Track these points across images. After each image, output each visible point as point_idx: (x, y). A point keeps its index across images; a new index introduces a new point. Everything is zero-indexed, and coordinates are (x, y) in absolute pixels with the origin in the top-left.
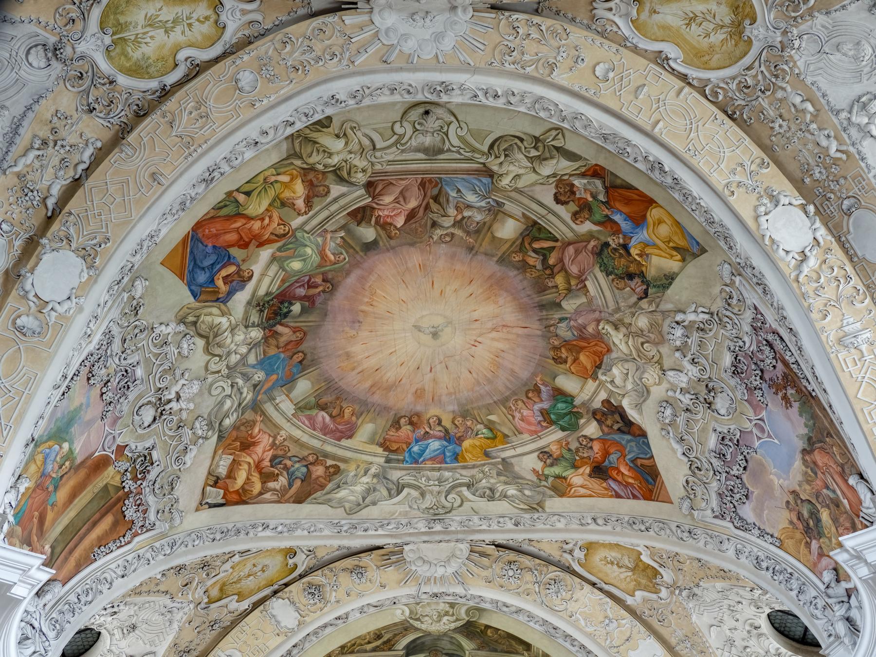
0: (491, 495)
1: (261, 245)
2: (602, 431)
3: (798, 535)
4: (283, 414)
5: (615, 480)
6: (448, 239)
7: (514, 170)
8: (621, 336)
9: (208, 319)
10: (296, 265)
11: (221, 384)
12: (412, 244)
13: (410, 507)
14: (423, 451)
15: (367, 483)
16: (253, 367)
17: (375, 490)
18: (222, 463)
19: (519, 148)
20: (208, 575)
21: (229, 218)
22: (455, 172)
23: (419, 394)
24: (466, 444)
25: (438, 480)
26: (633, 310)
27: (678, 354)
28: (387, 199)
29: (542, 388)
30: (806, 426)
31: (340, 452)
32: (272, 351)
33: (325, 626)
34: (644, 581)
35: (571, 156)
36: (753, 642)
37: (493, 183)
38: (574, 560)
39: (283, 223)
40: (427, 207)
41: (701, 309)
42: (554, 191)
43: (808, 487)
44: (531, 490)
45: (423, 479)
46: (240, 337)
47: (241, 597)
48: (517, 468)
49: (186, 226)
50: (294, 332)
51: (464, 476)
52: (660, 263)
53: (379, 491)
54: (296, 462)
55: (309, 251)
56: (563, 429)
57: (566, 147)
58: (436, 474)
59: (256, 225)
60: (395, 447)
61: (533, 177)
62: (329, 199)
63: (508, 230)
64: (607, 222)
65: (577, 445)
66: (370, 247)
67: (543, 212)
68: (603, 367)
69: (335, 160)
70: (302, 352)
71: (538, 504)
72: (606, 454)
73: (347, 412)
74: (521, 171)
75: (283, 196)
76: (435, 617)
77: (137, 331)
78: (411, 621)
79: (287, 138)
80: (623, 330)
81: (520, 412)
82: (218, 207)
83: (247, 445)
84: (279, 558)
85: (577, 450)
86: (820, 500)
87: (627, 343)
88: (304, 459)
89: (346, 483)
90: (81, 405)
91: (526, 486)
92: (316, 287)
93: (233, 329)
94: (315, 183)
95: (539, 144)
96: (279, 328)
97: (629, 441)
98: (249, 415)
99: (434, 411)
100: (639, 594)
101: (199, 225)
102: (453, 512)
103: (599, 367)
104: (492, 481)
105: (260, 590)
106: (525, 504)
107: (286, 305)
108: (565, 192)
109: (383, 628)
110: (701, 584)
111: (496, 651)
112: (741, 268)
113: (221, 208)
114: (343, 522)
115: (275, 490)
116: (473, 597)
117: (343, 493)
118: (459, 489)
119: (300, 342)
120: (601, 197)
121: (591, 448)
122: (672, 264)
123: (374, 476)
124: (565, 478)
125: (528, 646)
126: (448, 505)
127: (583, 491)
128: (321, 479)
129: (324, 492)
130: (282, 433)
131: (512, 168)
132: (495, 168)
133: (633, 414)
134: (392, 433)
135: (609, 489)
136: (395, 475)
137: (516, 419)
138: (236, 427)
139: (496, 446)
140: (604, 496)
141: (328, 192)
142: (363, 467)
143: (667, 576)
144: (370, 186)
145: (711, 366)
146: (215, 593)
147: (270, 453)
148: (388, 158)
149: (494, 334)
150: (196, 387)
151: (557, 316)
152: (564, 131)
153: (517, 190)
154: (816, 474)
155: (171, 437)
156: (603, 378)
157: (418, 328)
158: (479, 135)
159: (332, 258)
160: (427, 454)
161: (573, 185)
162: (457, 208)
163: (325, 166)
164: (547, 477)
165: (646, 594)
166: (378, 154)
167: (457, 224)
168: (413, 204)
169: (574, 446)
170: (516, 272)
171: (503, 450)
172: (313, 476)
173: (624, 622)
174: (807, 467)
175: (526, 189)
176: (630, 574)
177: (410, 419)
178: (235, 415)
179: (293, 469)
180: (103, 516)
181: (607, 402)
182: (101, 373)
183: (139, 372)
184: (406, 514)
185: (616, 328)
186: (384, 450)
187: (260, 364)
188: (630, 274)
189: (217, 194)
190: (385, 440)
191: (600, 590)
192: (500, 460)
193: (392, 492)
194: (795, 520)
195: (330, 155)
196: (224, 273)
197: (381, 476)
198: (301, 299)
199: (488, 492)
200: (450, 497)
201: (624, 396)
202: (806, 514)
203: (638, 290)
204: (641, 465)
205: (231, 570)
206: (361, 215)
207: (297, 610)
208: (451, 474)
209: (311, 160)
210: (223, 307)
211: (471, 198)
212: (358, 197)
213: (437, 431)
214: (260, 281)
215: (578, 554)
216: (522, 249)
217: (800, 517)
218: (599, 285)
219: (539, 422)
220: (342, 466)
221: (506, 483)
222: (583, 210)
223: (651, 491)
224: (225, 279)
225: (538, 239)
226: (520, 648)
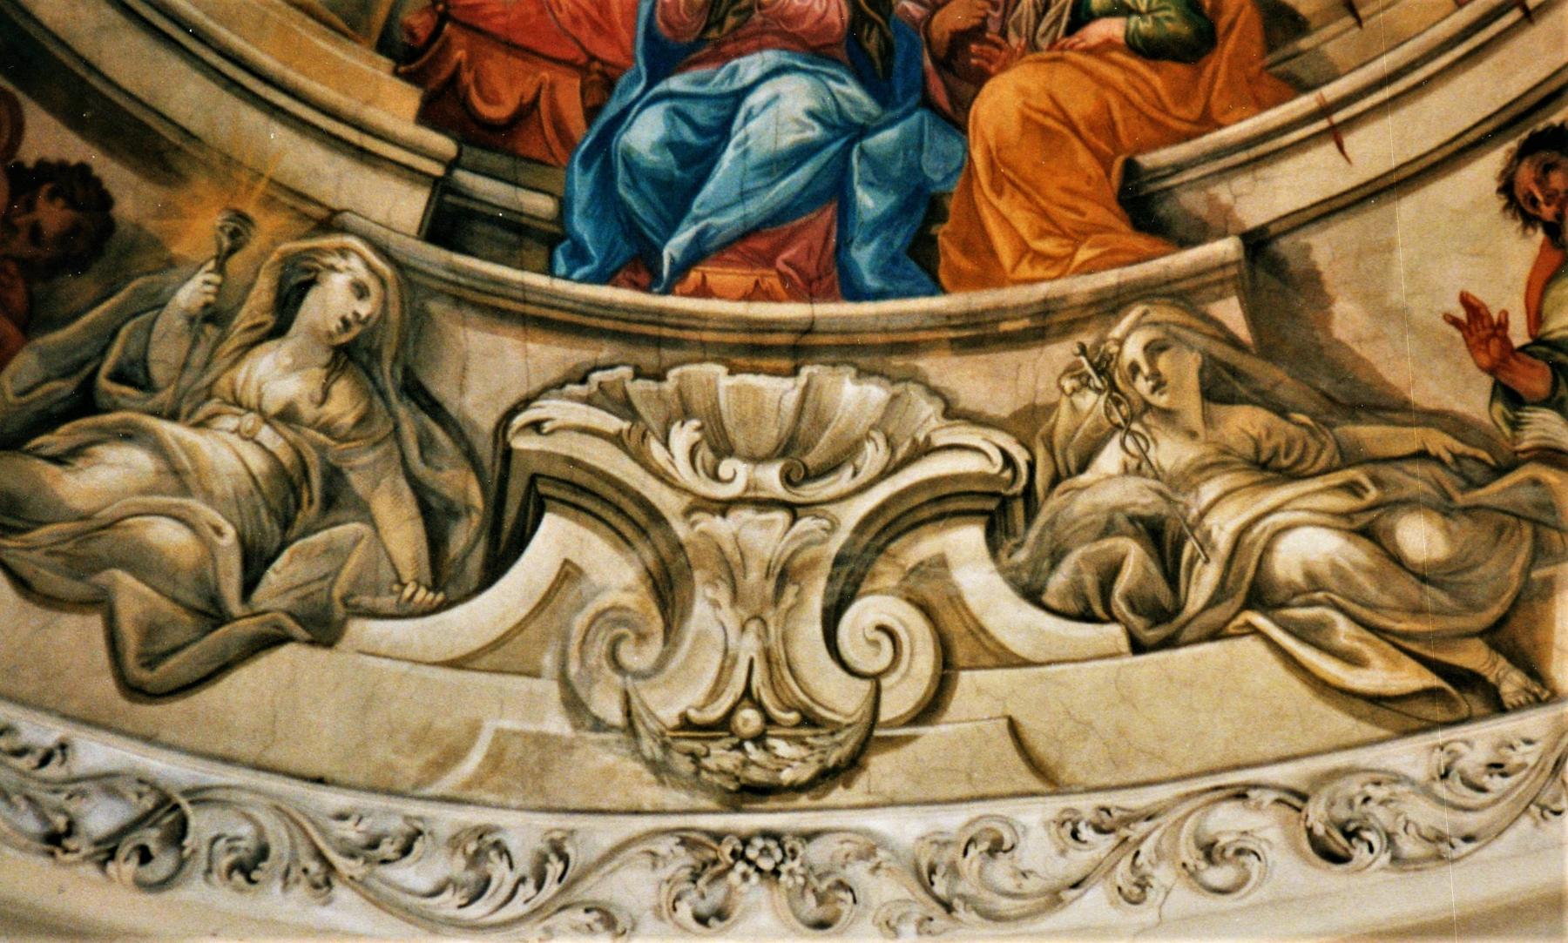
13: (574, 704)
14: (696, 159)
15: (287, 416)
17: (337, 497)
24: (1000, 103)
25: (787, 447)
44: (1445, 509)
45: (683, 436)
48: (1348, 319)
53: (364, 511)
58: (777, 392)
60: (501, 91)
71: (1496, 635)
91: (1416, 480)
102: (880, 765)
104: (1171, 452)
114: (96, 752)
117: (108, 475)
118: (926, 546)
123: (349, 355)
126: (841, 697)
139: (1207, 122)
142: (273, 236)
160: (723, 197)
171: (1259, 154)
184: (524, 767)
192: (1226, 248)
193: (461, 536)
199: (1134, 557)
208: (876, 393)
220: (131, 195)
221: (1269, 468)
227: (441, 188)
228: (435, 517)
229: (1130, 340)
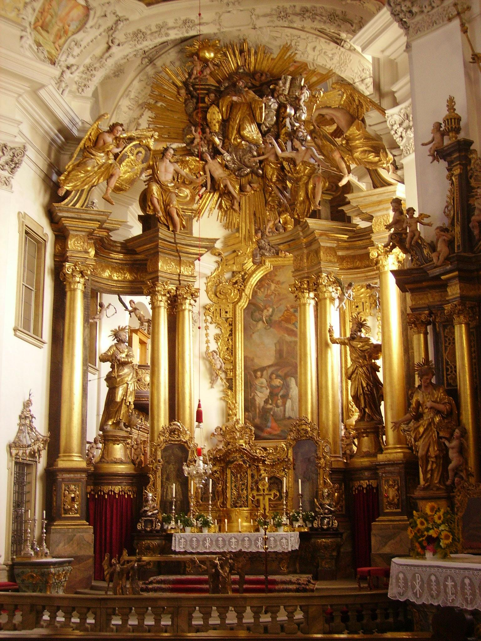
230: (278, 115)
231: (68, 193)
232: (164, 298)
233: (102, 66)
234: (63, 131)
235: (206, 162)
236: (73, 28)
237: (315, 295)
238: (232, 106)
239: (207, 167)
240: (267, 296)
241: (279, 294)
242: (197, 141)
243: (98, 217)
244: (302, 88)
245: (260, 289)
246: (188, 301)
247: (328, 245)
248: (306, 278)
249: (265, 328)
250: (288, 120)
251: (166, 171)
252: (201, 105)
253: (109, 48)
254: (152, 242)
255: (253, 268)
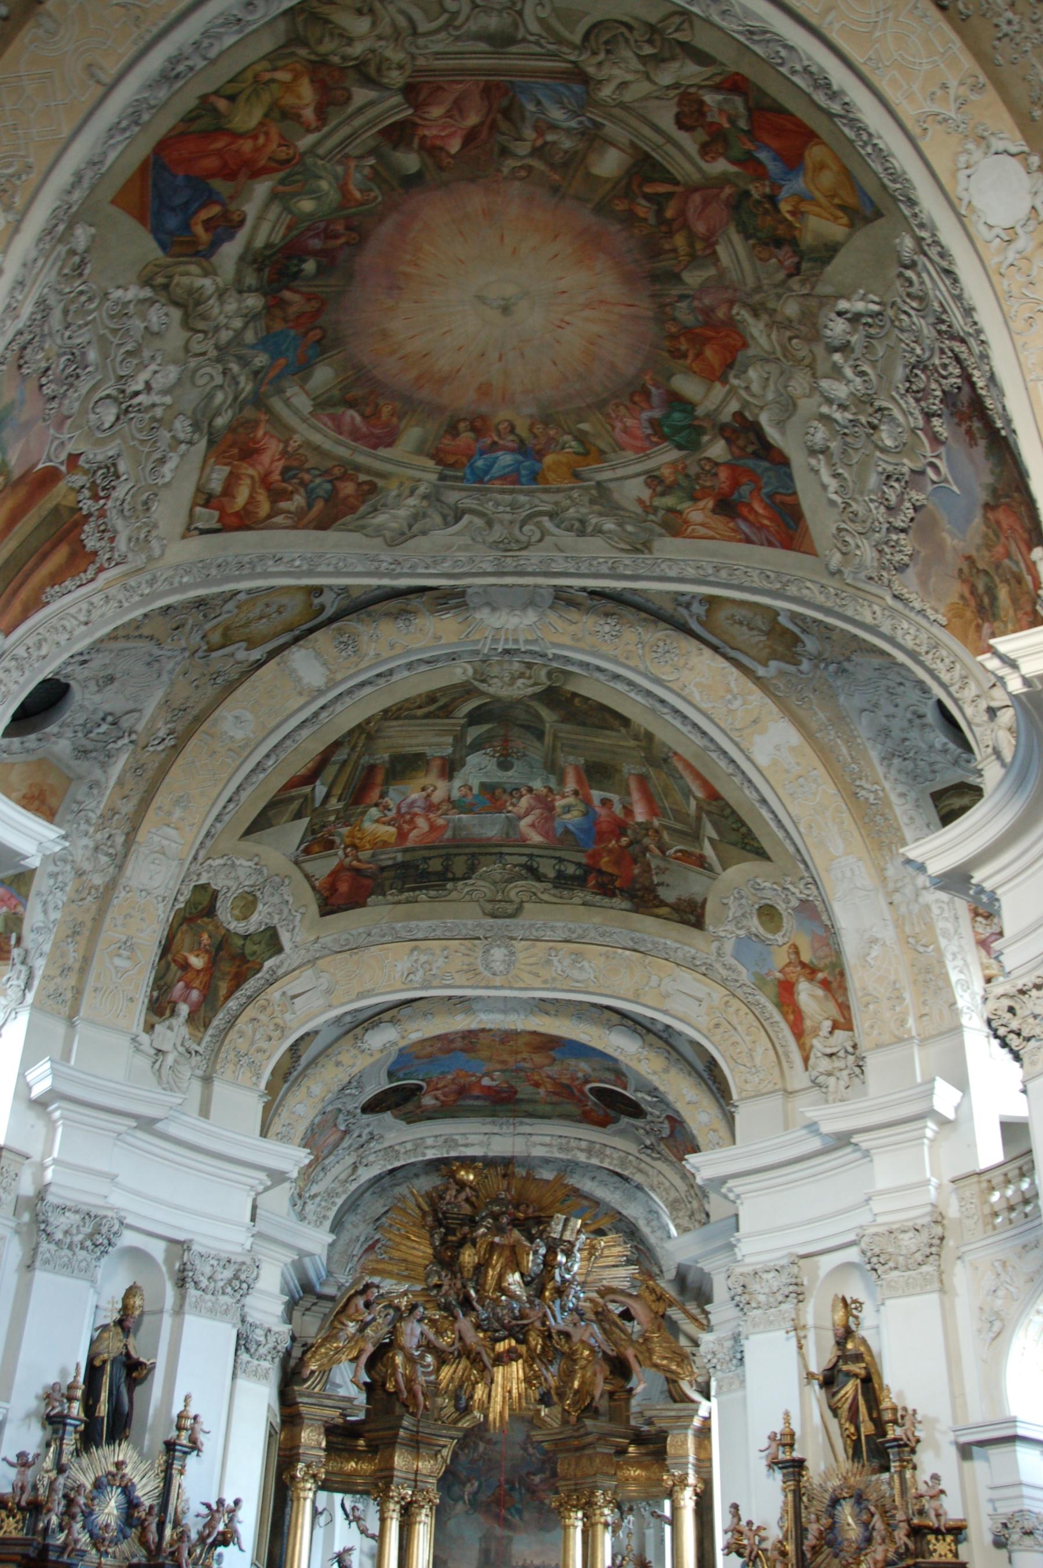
0: (581, 529)
1: (256, 174)
2: (732, 453)
3: (968, 614)
4: (296, 412)
5: (745, 519)
6: (523, 173)
7: (619, 74)
8: (761, 325)
9: (185, 280)
10: (307, 205)
11: (208, 370)
12: (472, 180)
13: (473, 539)
16: (253, 347)
17: (425, 515)
18: (214, 476)
19: (627, 41)
20: (205, 616)
21: (208, 135)
22: (534, 73)
23: (484, 390)
24: (549, 459)
26: (780, 290)
27: (837, 357)
28: (436, 112)
29: (653, 390)
30: (992, 473)
31: (377, 465)
32: (278, 326)
33: (363, 684)
34: (780, 649)
35: (702, 58)
36: (914, 734)
37: (588, 93)
38: (691, 616)
39: (285, 142)
40: (493, 127)
41: (872, 297)
42: (675, 110)
43: (987, 554)
46: (231, 307)
47: (252, 644)
48: (616, 496)
49: (143, 148)
50: (309, 300)
51: (545, 502)
52: (820, 226)
54: (316, 476)
55: (324, 185)
56: (680, 447)
57: (695, 43)
58: (508, 498)
59: (247, 146)
60: (451, 460)
61: (645, 87)
62: (350, 109)
63: (609, 164)
64: (749, 162)
65: (698, 469)
66: (412, 182)
67: (660, 140)
68: (736, 367)
69: (357, 49)
70: (320, 327)
72: (736, 484)
73: (386, 411)
74: (629, 77)
75: (283, 102)
76: (506, 679)
77: (83, 298)
78: (476, 683)
79: (285, 13)
80: (765, 317)
81: (621, 421)
82: (189, 118)
83: (249, 453)
84: (300, 597)
85: (698, 477)
86: (1000, 571)
87: (769, 336)
88: (327, 472)
89: (384, 505)
90: (13, 402)
92: (336, 236)
93: (221, 294)
94: (331, 83)
95: (656, 37)
96: (287, 295)
97: (766, 470)
98: (249, 413)
99: (504, 414)
100: (773, 664)
101: (162, 146)
103: (730, 366)
104: (583, 510)
105: (276, 635)
106: (627, 543)
107: (295, 262)
108: (690, 113)
109: (440, 690)
110: (853, 657)
111: (584, 724)
112: (930, 245)
113: (192, 120)
115: (289, 512)
116: (556, 657)
117: (381, 519)
118: (538, 519)
119: (317, 313)
120: (743, 124)
121: (716, 475)
122: (835, 230)
124: (680, 513)
125: (626, 722)
126: (524, 539)
127: (702, 531)
128: (352, 500)
129: (356, 516)
130: (296, 437)
131: (616, 71)
132: (591, 70)
133: (772, 434)
134: (446, 442)
135: (737, 530)
136: (452, 497)
137: (617, 430)
138: (231, 428)
140: (730, 539)
141: (349, 98)
143: (811, 644)
144: (409, 91)
145: (880, 377)
146: (216, 638)
147: (281, 464)
148: (436, 48)
149: (588, 313)
150: (172, 373)
151: (675, 291)
152: (694, 18)
153: (623, 106)
154: (997, 536)
155: (142, 442)
156: (735, 382)
157: (481, 299)
158: (568, 17)
159: (358, 195)
160: (495, 471)
161: (702, 103)
162: (536, 128)
163: (344, 58)
164: (655, 510)
165: (782, 665)
166: (421, 41)
167: (537, 152)
168: (473, 120)
169: (693, 470)
170: (618, 227)
172: (342, 495)
173: (751, 698)
174: (988, 527)
175: (636, 105)
176: (763, 638)
177: (472, 423)
178: (230, 413)
179: (312, 485)
180: (55, 546)
181: (739, 415)
182: (37, 359)
183: (92, 355)
185: (756, 315)
186: (437, 464)
187: (262, 343)
188: (776, 239)
189: (188, 101)
190: (438, 450)
191: (725, 656)
194: (967, 594)
195: (350, 41)
196: (204, 215)
197: (433, 497)
198: (315, 253)
199: (577, 525)
200: (526, 528)
201: (762, 408)
202: (981, 588)
203: (787, 263)
204: (782, 503)
205: (236, 611)
206: (398, 134)
207: (325, 664)
208: (527, 498)
209: (323, 49)
210: (205, 264)
211: (556, 114)
212: (393, 108)
213: (509, 441)
214: (255, 228)
215: (697, 608)
216: (627, 194)
217: (973, 591)
218: (733, 252)
219: (648, 436)
221: (601, 514)
222: (716, 142)
223: (792, 538)
224: (207, 224)
225: (650, 181)
226: (616, 723)
227: (440, 473)
228: (444, 517)
229: (575, 494)
230: (545, 1263)
231: (313, 1372)
232: (398, 1507)
233: (344, 1192)
234: (307, 1288)
235: (456, 1318)
236: (326, 1152)
237: (585, 1515)
238: (492, 1247)
239: (457, 1326)
240: (473, 1461)
241: (490, 1460)
242: (445, 1288)
243: (342, 1404)
244: (579, 1232)
245: (462, 1449)
246: (424, 1511)
247: (606, 1451)
248: (576, 1490)
249: (467, 1513)
250: (557, 1271)
251: (412, 1334)
252: (450, 1238)
253: (355, 1167)
254: (389, 1429)
255: (455, 1415)
